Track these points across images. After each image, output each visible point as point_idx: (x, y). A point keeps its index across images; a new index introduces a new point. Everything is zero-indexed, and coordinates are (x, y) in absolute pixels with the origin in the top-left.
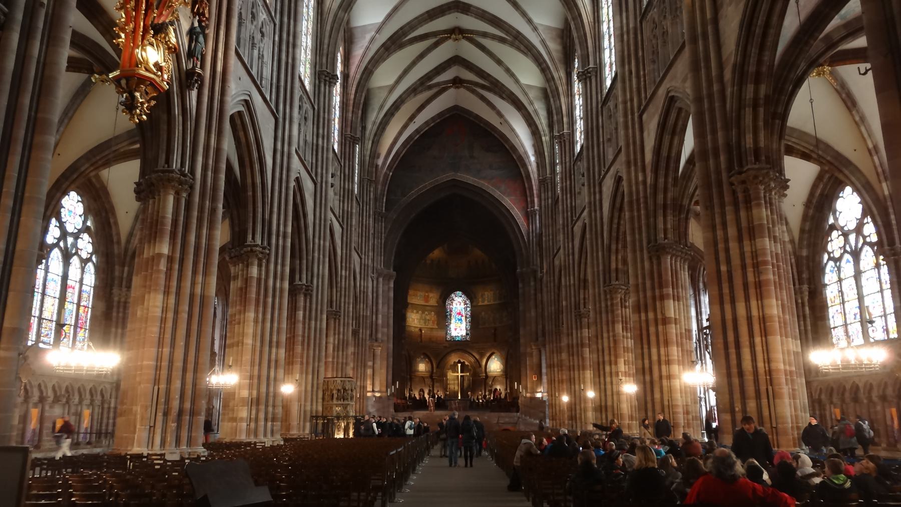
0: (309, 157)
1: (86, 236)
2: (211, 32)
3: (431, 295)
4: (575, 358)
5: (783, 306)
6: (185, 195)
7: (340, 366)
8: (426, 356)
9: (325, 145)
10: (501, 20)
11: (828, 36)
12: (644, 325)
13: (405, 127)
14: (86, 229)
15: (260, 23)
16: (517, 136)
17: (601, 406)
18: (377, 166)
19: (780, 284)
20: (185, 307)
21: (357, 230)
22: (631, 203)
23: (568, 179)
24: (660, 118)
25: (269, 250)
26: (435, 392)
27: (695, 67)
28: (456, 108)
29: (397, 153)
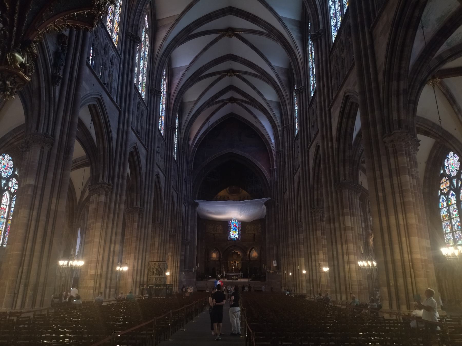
0: (143, 136)
1: (14, 180)
4: (296, 250)
6: (47, 149)
7: (162, 254)
9: (154, 129)
10: (254, 64)
11: (440, 56)
14: (14, 176)
15: (110, 57)
16: (265, 129)
17: (310, 279)
18: (189, 145)
20: (43, 218)
21: (176, 178)
23: (291, 150)
24: (341, 109)
25: (113, 186)
26: (221, 269)
27: (361, 75)
28: (232, 114)
29: (200, 138)
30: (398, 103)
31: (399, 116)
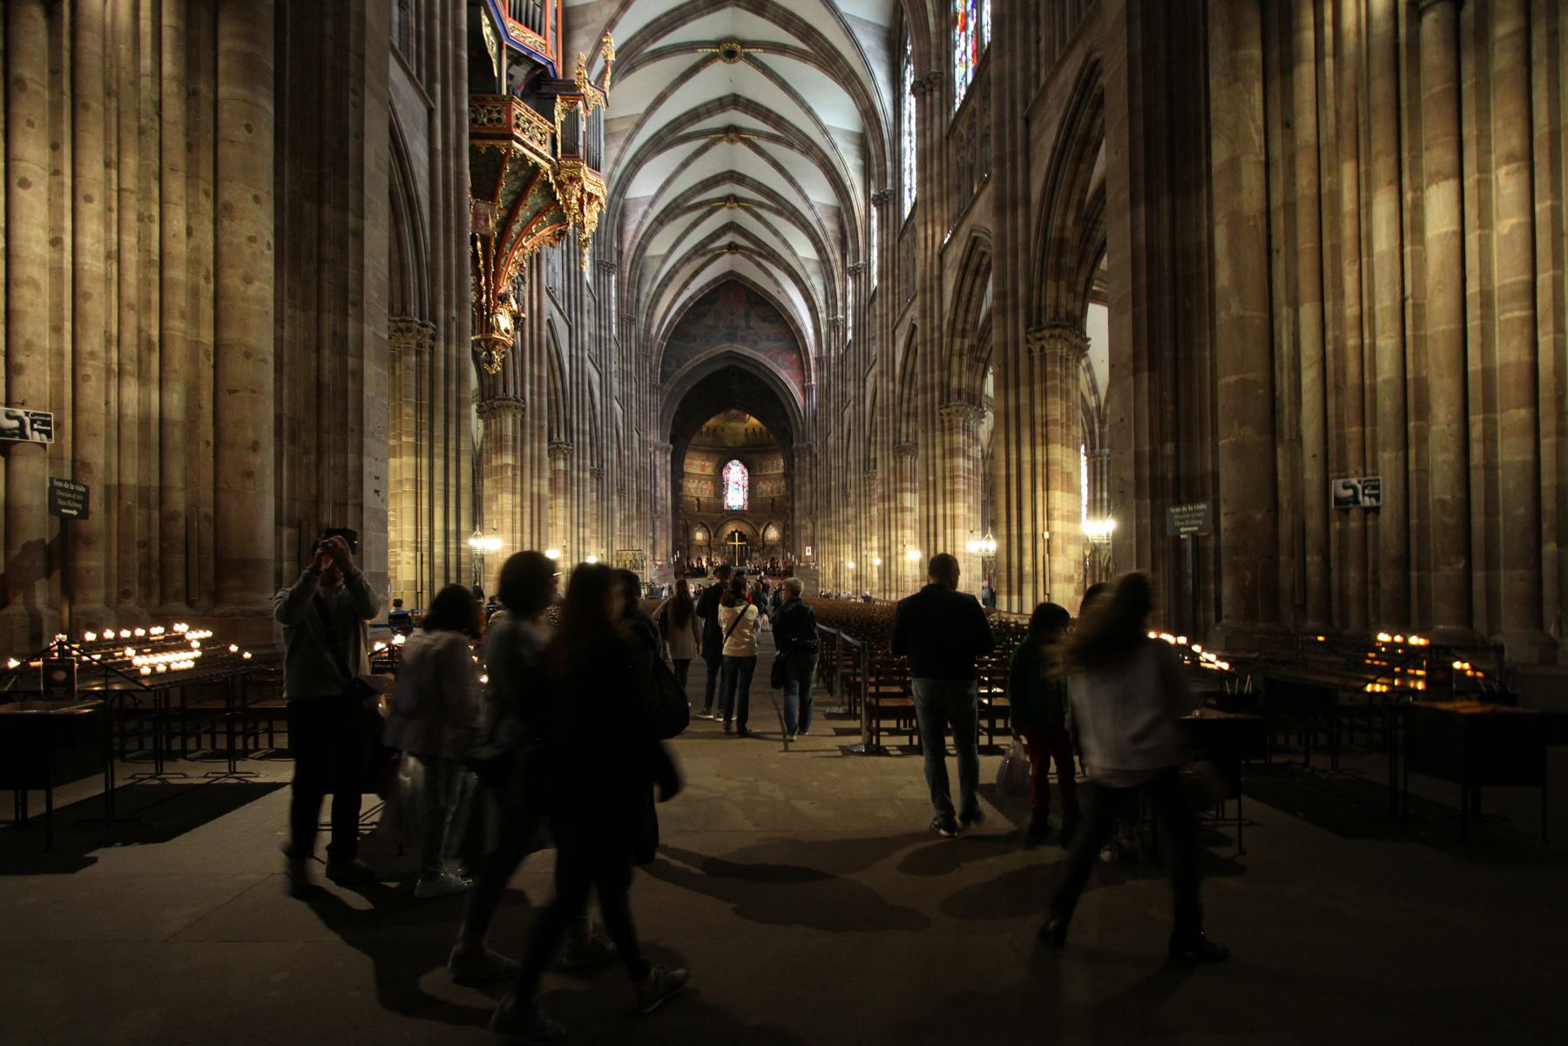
0: (593, 350)
2: (527, 280)
3: (707, 464)
5: (969, 507)
8: (704, 525)
10: (778, 194)
12: (887, 512)
13: (678, 294)
19: (969, 491)
22: (882, 408)
27: (924, 317)
28: (731, 273)
29: (670, 321)
30: (960, 366)
31: (960, 383)
